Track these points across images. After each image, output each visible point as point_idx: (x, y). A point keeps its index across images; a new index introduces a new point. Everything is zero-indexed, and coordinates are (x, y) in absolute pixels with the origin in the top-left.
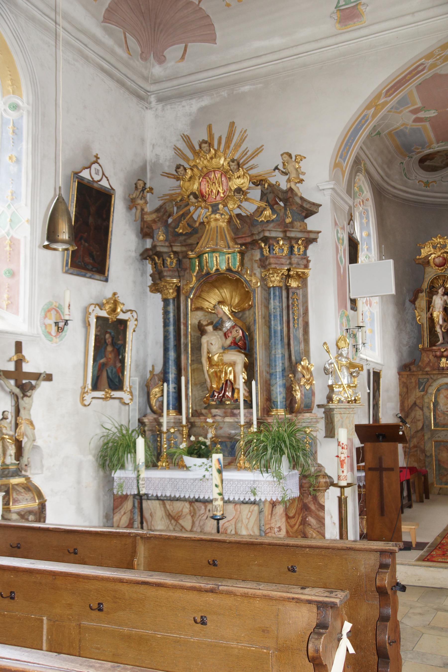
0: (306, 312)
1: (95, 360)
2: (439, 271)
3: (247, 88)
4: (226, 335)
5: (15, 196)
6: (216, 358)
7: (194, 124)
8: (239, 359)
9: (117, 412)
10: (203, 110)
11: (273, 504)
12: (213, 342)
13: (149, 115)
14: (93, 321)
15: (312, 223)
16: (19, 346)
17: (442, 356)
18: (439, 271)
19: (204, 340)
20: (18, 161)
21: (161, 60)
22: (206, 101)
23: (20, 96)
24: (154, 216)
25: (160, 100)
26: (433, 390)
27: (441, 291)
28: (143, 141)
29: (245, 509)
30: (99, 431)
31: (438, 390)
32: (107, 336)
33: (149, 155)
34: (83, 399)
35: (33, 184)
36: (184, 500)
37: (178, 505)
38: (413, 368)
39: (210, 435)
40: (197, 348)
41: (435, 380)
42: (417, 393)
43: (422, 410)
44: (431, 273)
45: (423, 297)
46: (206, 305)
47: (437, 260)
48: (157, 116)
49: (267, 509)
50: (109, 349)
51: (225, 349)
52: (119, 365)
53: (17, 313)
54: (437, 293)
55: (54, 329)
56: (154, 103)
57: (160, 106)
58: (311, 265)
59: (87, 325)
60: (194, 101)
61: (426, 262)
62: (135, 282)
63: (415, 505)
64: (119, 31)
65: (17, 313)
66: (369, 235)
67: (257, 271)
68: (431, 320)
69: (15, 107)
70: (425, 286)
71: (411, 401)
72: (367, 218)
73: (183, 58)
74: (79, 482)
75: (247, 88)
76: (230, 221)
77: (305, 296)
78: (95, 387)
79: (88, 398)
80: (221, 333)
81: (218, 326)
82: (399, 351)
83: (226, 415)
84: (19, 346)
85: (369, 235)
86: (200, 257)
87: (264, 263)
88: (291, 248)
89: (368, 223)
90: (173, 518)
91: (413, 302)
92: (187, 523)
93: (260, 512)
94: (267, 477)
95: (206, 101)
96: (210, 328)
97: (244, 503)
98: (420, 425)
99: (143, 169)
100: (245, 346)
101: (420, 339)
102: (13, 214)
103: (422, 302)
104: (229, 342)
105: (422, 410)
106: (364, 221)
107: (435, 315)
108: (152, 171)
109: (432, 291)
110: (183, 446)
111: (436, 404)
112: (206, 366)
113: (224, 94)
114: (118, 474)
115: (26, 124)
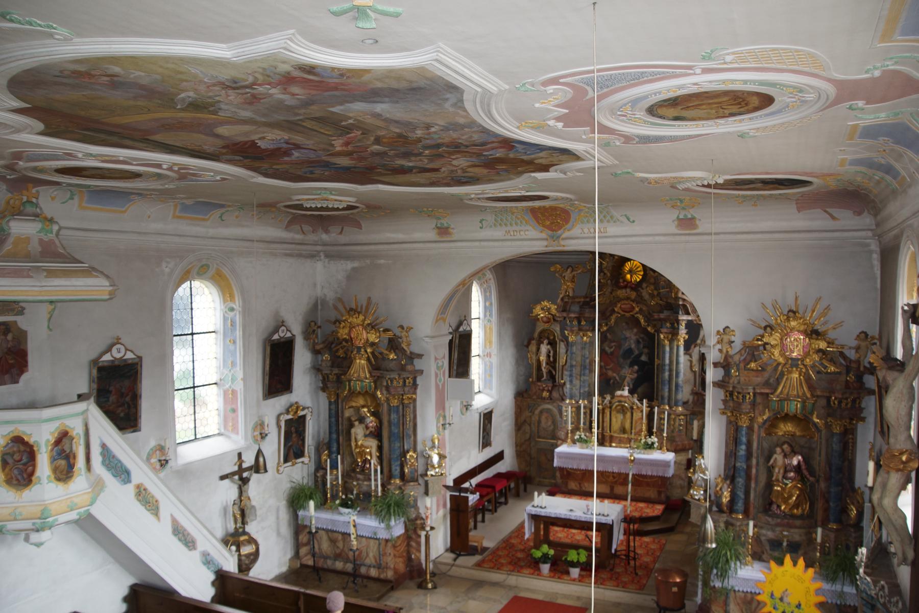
0: (415, 417)
1: (285, 445)
2: (546, 326)
3: (382, 261)
4: (367, 428)
5: (233, 364)
6: (359, 443)
7: (349, 278)
8: (373, 444)
9: (300, 472)
10: (353, 269)
11: (387, 541)
12: (358, 431)
13: (319, 265)
14: (283, 424)
15: (418, 364)
16: (240, 455)
17: (543, 390)
18: (546, 326)
19: (353, 431)
20: (234, 342)
21: (327, 231)
22: (356, 264)
23: (235, 302)
24: (321, 346)
25: (327, 256)
26: (537, 412)
27: (546, 342)
28: (315, 285)
29: (372, 542)
30: (289, 485)
31: (541, 412)
32: (293, 429)
33: (319, 292)
34: (278, 471)
35: (244, 356)
36: (338, 532)
37: (336, 535)
38: (525, 395)
39: (355, 492)
40: (349, 434)
41: (539, 406)
42: (527, 413)
43: (530, 425)
44: (540, 327)
45: (534, 342)
46: (354, 404)
47: (545, 319)
48: (325, 267)
49: (383, 543)
50: (294, 435)
51: (366, 436)
52: (300, 442)
53: (238, 433)
54: (543, 343)
55: (259, 437)
56: (322, 257)
57: (327, 260)
58: (418, 391)
59: (279, 427)
60: (348, 262)
61: (536, 319)
62: (310, 384)
63: (510, 501)
64: (297, 227)
65: (238, 433)
66: (491, 304)
67: (385, 392)
68: (539, 361)
69: (232, 309)
70: (536, 335)
71: (523, 418)
72: (490, 292)
73: (341, 233)
74: (278, 518)
75: (382, 261)
76: (368, 359)
77: (415, 407)
78: (286, 460)
79: (281, 469)
80: (363, 425)
81: (362, 420)
82: (517, 382)
83: (365, 480)
84: (240, 455)
85: (491, 304)
86: (350, 381)
87: (387, 388)
88: (405, 382)
89: (490, 295)
90: (333, 541)
91: (527, 346)
92: (340, 545)
93: (380, 544)
94: (383, 525)
95: (356, 264)
96: (357, 423)
97: (371, 538)
98: (528, 436)
99: (315, 305)
100: (377, 434)
101: (530, 376)
102: (233, 375)
103: (533, 348)
104: (368, 432)
105: (530, 425)
106: (488, 294)
107: (541, 358)
108: (322, 305)
109: (540, 343)
110: (338, 502)
111: (539, 422)
112: (353, 444)
113: (368, 262)
114: (301, 513)
115: (238, 319)
